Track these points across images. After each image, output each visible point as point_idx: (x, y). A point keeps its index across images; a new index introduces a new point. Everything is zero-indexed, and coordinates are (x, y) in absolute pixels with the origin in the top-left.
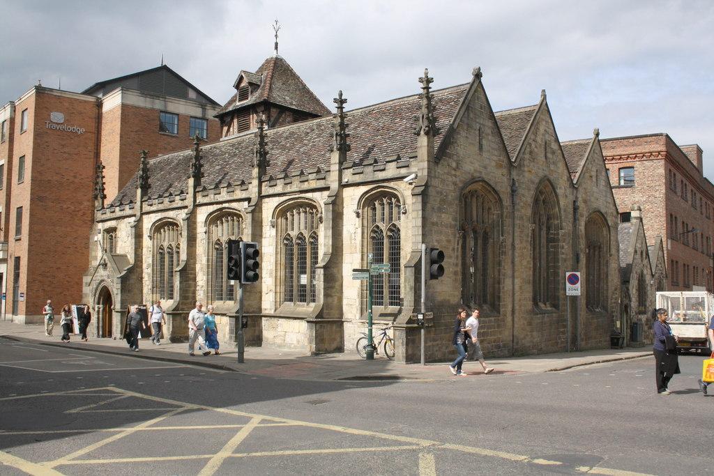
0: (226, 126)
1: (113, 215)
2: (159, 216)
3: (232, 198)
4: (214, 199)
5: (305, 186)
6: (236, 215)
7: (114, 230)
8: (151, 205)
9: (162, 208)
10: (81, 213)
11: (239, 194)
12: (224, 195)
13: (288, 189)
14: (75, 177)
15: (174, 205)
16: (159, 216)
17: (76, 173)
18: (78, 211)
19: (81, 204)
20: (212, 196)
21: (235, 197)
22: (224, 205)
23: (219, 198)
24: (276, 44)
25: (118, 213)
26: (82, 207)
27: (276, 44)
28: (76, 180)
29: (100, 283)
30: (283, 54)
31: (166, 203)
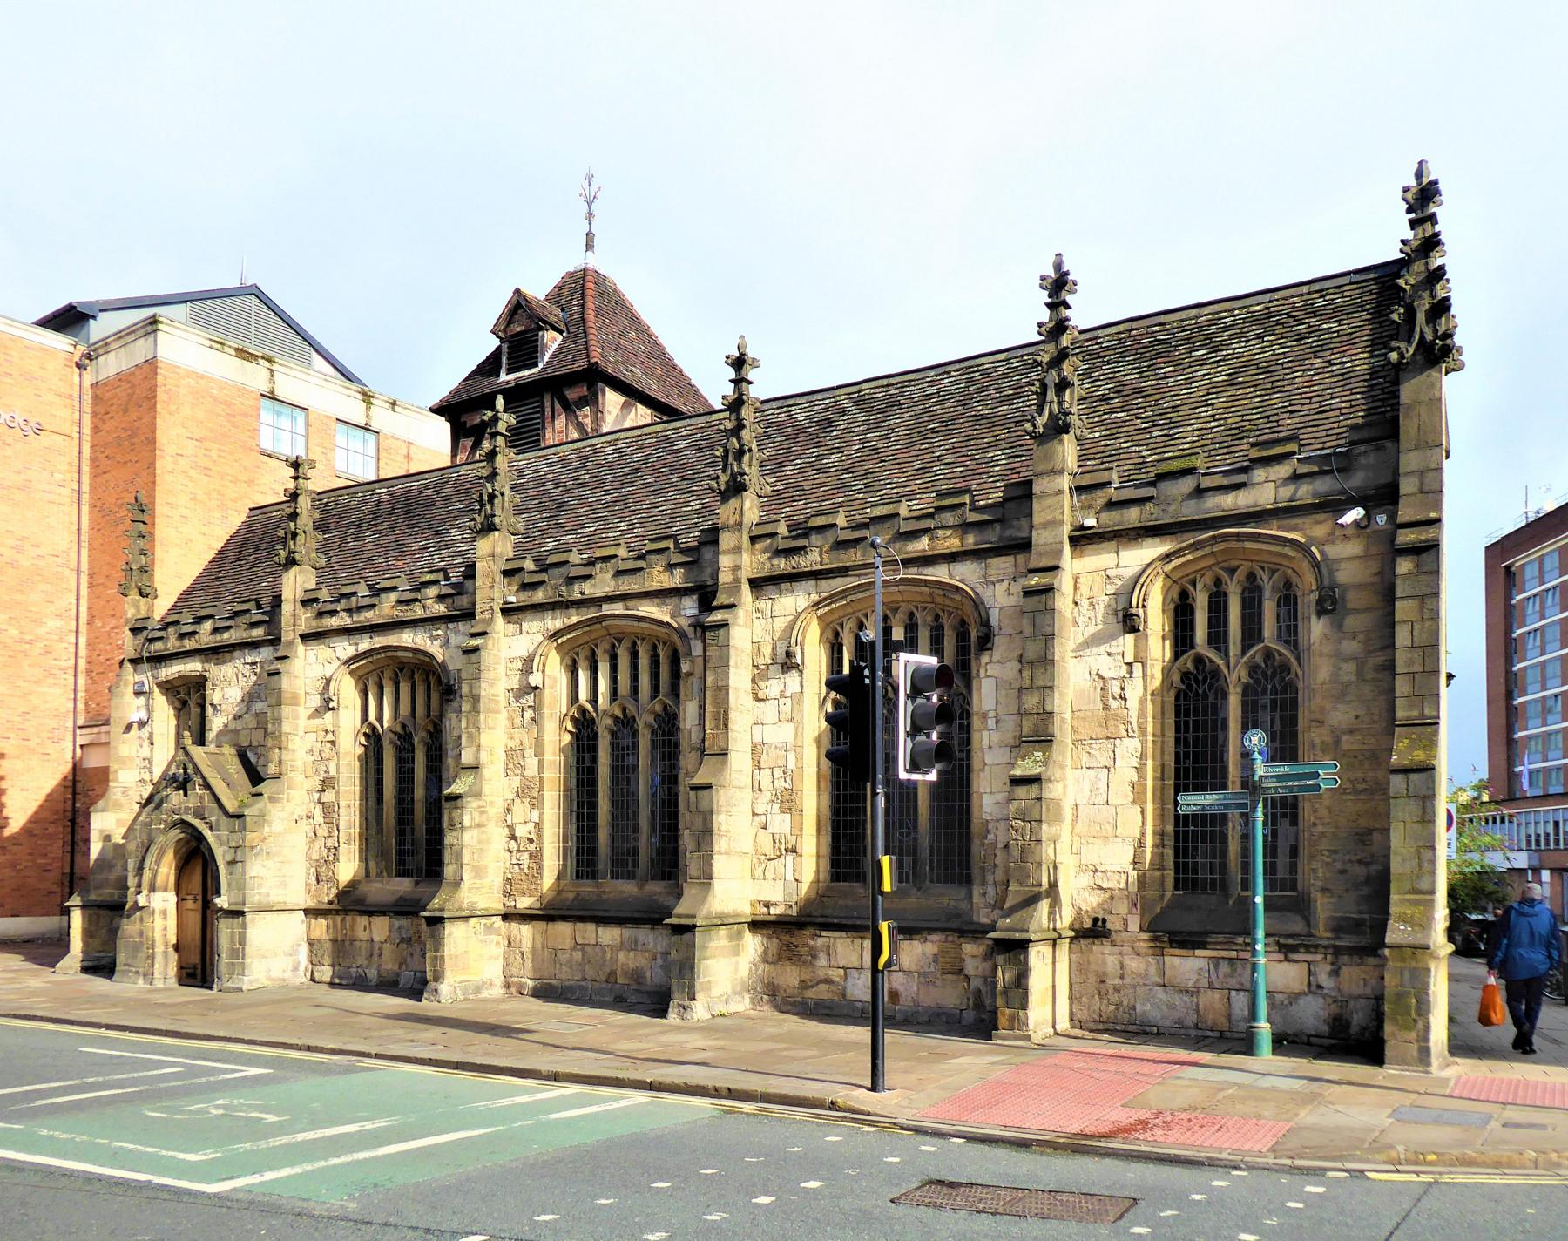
0: (467, 436)
1: (189, 644)
2: (365, 644)
7: (198, 684)
10: (38, 648)
14: (19, 549)
16: (365, 644)
17: (23, 539)
18: (31, 642)
19: (39, 622)
21: (655, 586)
22: (607, 609)
23: (588, 589)
26: (42, 631)
28: (26, 562)
31: (387, 608)
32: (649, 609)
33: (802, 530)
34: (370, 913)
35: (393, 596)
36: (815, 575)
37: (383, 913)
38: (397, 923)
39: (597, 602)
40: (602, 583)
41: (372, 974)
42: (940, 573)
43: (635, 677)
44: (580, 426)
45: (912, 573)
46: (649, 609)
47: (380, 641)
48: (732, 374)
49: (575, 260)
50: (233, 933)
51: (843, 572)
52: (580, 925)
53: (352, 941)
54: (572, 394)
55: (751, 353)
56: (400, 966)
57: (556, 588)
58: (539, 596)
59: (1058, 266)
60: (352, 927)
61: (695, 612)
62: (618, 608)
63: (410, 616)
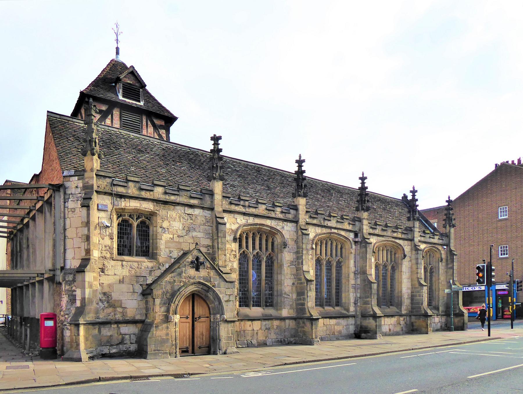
2: (251, 220)
3: (341, 227)
5: (395, 235)
9: (256, 213)
12: (333, 223)
13: (385, 233)
15: (273, 215)
21: (345, 228)
22: (333, 231)
23: (330, 224)
31: (261, 209)
32: (343, 233)
33: (376, 224)
34: (252, 320)
35: (264, 207)
36: (378, 235)
37: (259, 320)
38: (264, 323)
39: (331, 228)
40: (333, 223)
41: (254, 342)
42: (397, 241)
43: (331, 251)
44: (160, 135)
45: (393, 240)
46: (343, 233)
47: (258, 221)
48: (360, 181)
49: (113, 56)
50: (228, 330)
51: (383, 236)
52: (325, 319)
53: (244, 331)
54: (158, 122)
56: (266, 337)
57: (320, 221)
58: (315, 221)
59: (414, 188)
60: (244, 326)
61: (353, 237)
62: (336, 231)
63: (270, 215)
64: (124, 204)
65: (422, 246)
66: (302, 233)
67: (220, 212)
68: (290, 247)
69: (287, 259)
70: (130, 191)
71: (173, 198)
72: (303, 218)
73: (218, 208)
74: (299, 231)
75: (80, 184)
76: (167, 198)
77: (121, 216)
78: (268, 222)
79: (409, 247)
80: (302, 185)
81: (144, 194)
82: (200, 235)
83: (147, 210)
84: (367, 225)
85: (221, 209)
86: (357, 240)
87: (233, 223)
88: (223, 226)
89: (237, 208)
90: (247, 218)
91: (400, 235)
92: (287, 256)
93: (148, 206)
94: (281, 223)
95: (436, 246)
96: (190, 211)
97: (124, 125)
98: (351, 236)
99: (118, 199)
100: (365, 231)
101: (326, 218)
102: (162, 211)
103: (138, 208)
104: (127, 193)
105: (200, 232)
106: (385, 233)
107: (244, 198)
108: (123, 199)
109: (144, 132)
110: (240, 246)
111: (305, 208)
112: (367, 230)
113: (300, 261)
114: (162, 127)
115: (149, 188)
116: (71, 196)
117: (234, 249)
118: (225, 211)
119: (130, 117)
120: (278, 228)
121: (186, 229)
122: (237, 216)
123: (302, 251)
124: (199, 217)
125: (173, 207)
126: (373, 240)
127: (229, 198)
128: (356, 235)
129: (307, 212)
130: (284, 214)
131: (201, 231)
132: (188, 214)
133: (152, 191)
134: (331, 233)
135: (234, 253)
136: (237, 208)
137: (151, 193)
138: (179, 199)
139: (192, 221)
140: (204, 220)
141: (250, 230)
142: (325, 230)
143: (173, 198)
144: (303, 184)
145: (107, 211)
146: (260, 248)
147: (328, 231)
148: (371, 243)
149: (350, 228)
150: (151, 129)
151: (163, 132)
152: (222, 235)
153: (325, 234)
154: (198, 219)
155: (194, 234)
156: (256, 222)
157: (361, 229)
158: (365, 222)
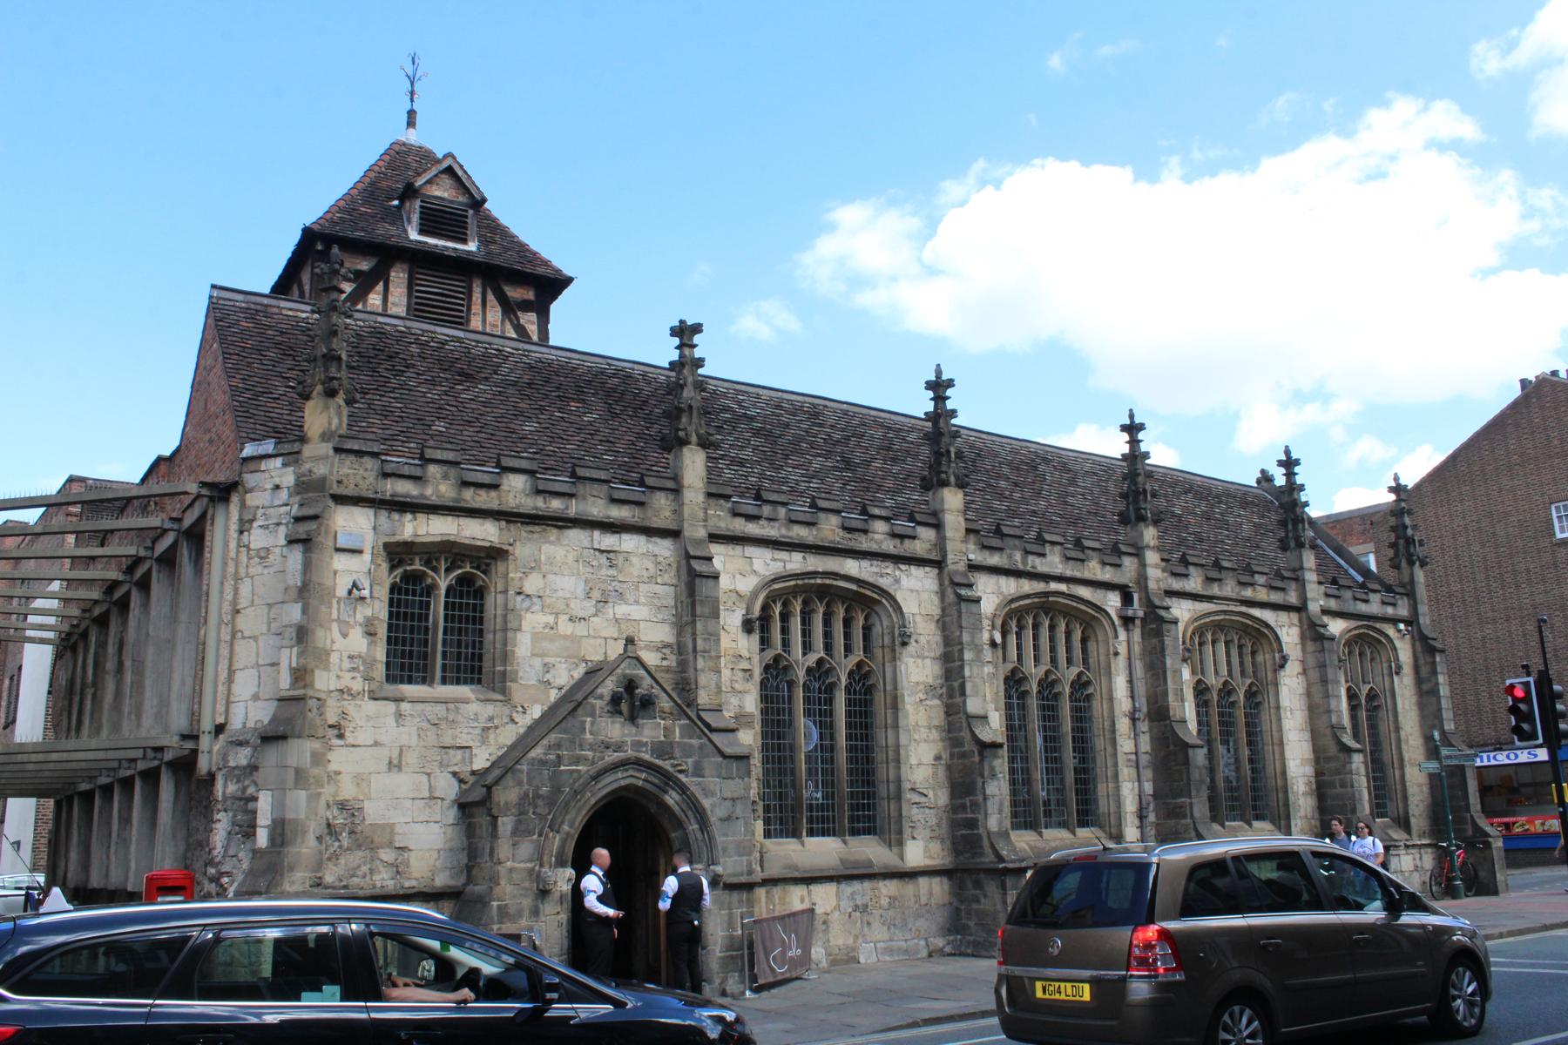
2: (796, 562)
3: (1078, 574)
4: (1024, 562)
5: (1248, 593)
6: (1088, 620)
8: (750, 518)
9: (811, 540)
11: (1094, 569)
12: (1053, 562)
13: (1215, 590)
15: (864, 544)
16: (796, 562)
20: (1018, 556)
21: (1087, 575)
22: (1054, 586)
23: (1041, 565)
24: (411, 114)
25: (515, 490)
27: (411, 114)
29: (597, 777)
30: (431, 137)
31: (829, 529)
33: (1184, 561)
35: (834, 520)
40: (1053, 562)
42: (1256, 612)
43: (1053, 649)
44: (520, 329)
45: (1243, 609)
46: (1084, 592)
51: (1210, 599)
54: (515, 293)
55: (1294, 456)
57: (1010, 557)
58: (994, 560)
62: (1063, 587)
64: (413, 528)
65: (1336, 627)
66: (959, 596)
67: (698, 543)
68: (923, 640)
69: (914, 679)
70: (429, 491)
71: (556, 504)
72: (961, 550)
73: (695, 531)
74: (949, 591)
75: (288, 478)
76: (539, 504)
77: (401, 563)
78: (851, 567)
79: (1295, 631)
80: (948, 452)
81: (471, 497)
82: (639, 612)
83: (479, 543)
84: (1156, 566)
85: (702, 533)
86: (1130, 613)
87: (742, 574)
88: (711, 582)
89: (752, 529)
90: (784, 555)
91: (1262, 595)
92: (917, 671)
93: (483, 532)
94: (889, 568)
95: (1378, 625)
96: (608, 541)
97: (417, 309)
98: (1112, 602)
99: (396, 516)
100: (1152, 585)
101: (1029, 547)
102: (526, 547)
103: (452, 538)
104: (422, 496)
105: (637, 602)
106: (1215, 590)
107: (774, 497)
108: (409, 516)
109: (476, 323)
110: (765, 642)
111: (961, 519)
112: (1158, 581)
113: (956, 684)
114: (526, 306)
115: (486, 479)
116: (260, 512)
117: (745, 653)
118: (714, 538)
119: (433, 285)
120: (884, 582)
121: (596, 595)
122: (752, 551)
123: (961, 651)
124: (634, 560)
125: (555, 531)
126: (1182, 611)
127: (727, 497)
128: (1127, 599)
129: (968, 531)
130: (897, 541)
131: (642, 600)
132: (602, 551)
133: (496, 487)
134: (1047, 594)
135: (745, 665)
136: (752, 529)
137: (493, 494)
138: (573, 508)
139: (612, 572)
140: (651, 566)
141: (795, 591)
142: (1027, 586)
143: (556, 504)
144: (952, 450)
145: (360, 552)
146: (828, 647)
147: (1039, 586)
148: (1175, 622)
149: (1107, 575)
150: (495, 314)
151: (529, 320)
152: (707, 610)
153: (1028, 596)
154: (632, 565)
155: (621, 610)
156: (810, 569)
157: (1142, 579)
158: (1152, 557)
